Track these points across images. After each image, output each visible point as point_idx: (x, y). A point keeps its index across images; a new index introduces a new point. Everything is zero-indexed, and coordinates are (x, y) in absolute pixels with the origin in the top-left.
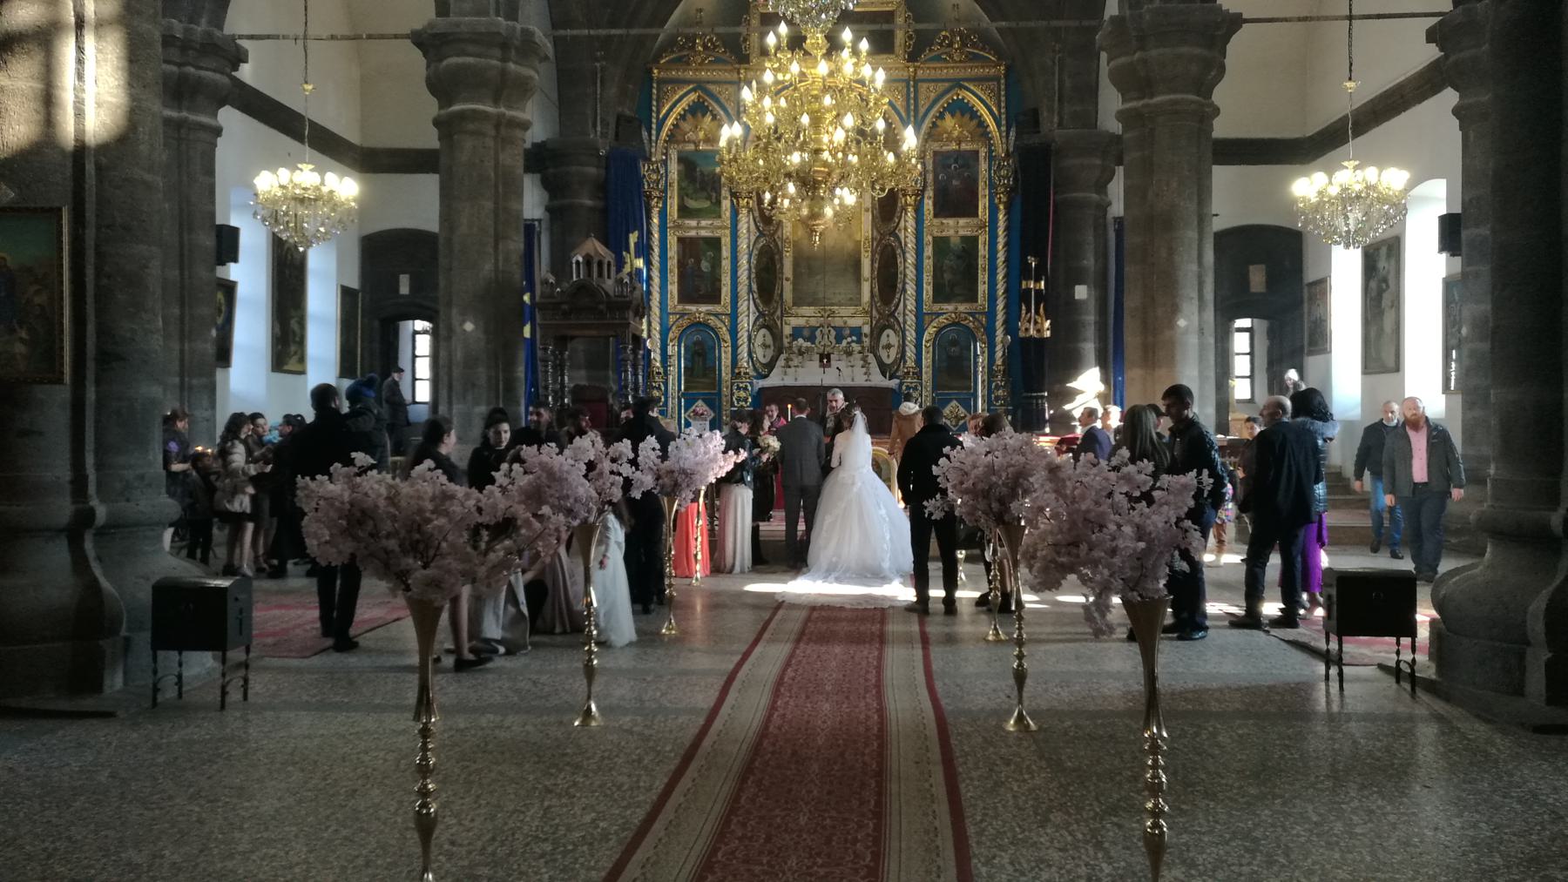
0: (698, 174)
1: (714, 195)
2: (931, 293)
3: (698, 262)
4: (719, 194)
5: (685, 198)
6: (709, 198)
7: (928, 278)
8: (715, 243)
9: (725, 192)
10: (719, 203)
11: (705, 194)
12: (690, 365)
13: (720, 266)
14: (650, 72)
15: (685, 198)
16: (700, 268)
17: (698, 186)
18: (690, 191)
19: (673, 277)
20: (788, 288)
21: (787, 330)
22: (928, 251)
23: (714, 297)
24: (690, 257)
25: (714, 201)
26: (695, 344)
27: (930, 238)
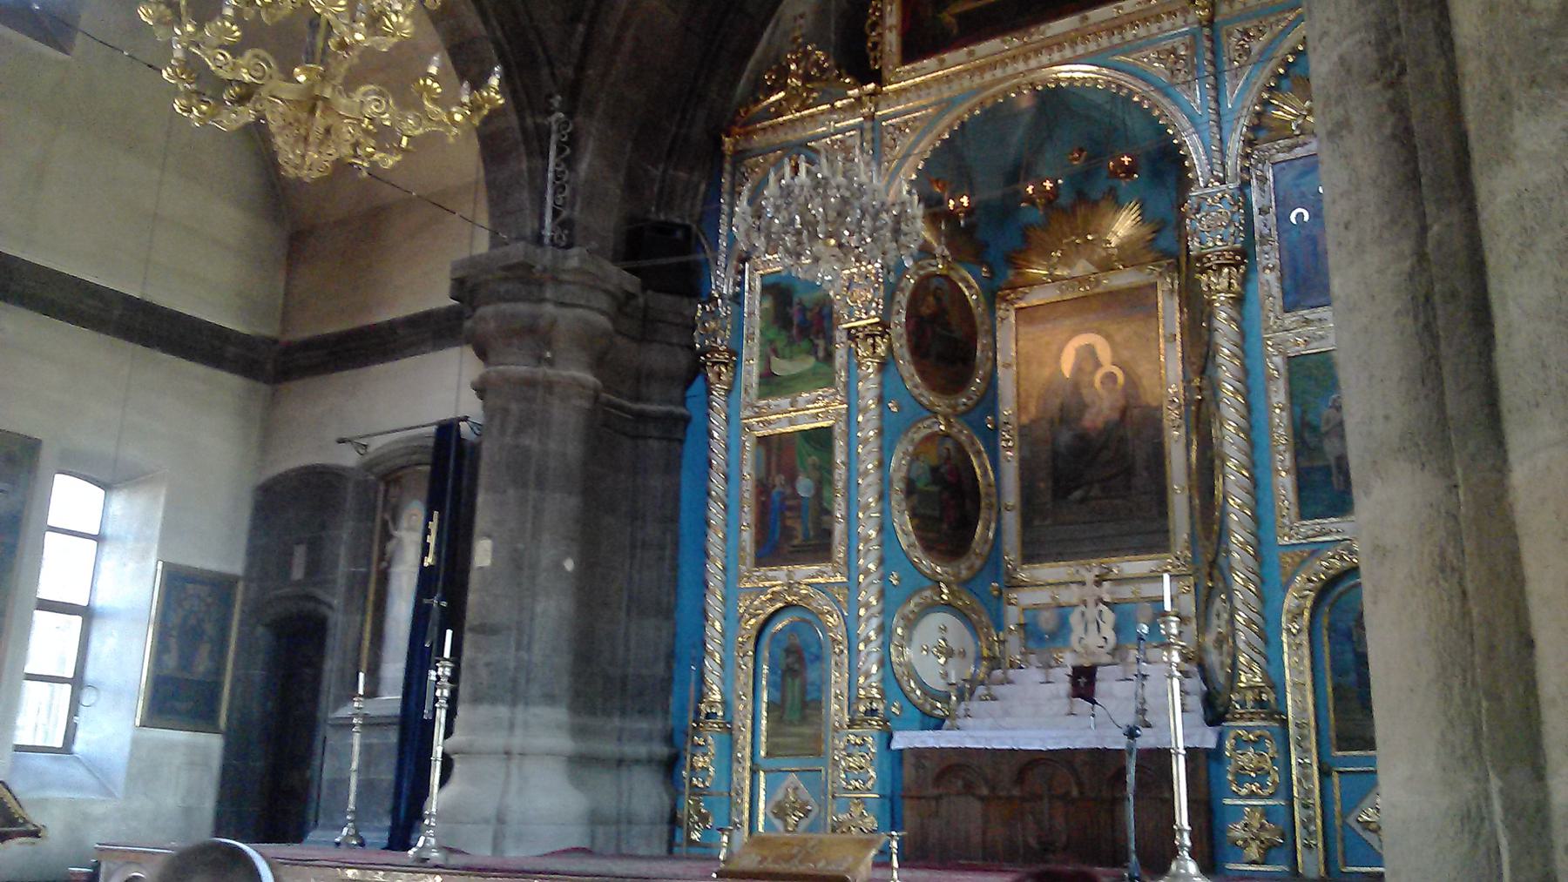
0: (796, 308)
1: (821, 343)
2: (1292, 496)
3: (792, 479)
4: (830, 340)
5: (774, 359)
6: (813, 351)
7: (1283, 459)
8: (821, 439)
9: (840, 336)
10: (829, 357)
11: (805, 344)
12: (777, 695)
13: (831, 483)
14: (720, 143)
15: (774, 359)
16: (796, 496)
17: (794, 331)
18: (780, 345)
19: (748, 517)
20: (1012, 521)
21: (1013, 616)
22: (1279, 396)
23: (818, 547)
24: (779, 471)
25: (821, 354)
26: (788, 651)
27: (1278, 360)
